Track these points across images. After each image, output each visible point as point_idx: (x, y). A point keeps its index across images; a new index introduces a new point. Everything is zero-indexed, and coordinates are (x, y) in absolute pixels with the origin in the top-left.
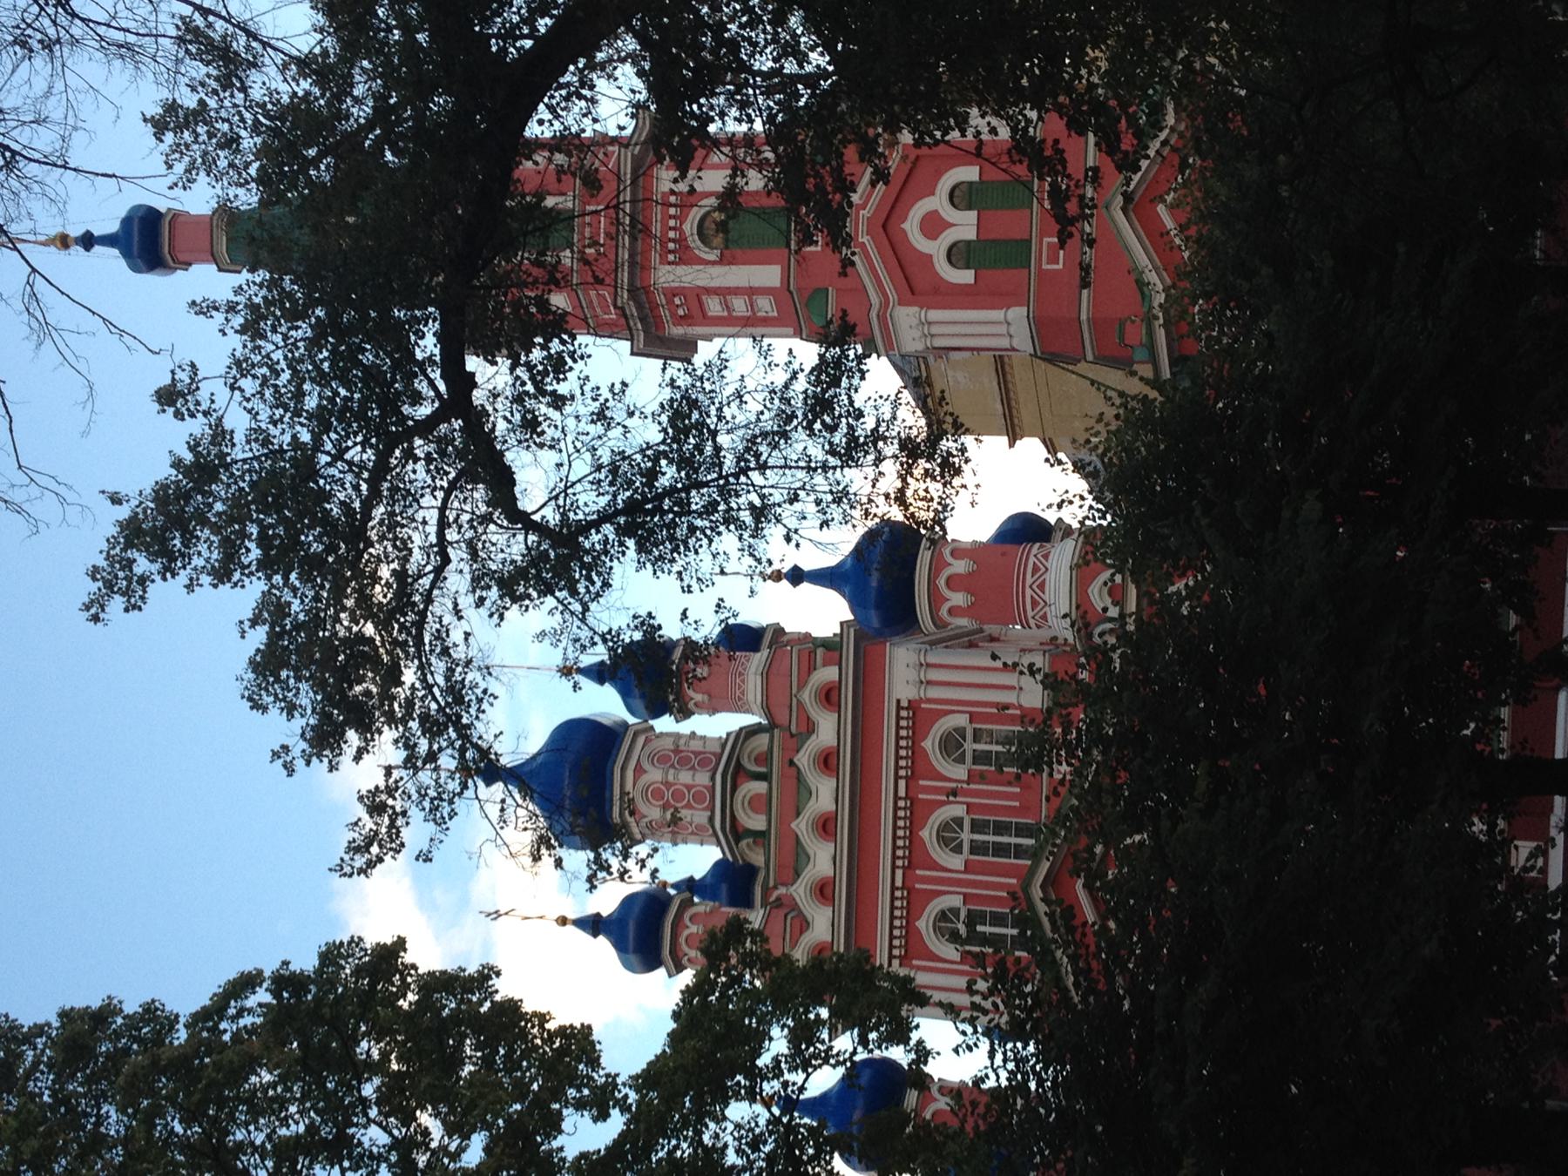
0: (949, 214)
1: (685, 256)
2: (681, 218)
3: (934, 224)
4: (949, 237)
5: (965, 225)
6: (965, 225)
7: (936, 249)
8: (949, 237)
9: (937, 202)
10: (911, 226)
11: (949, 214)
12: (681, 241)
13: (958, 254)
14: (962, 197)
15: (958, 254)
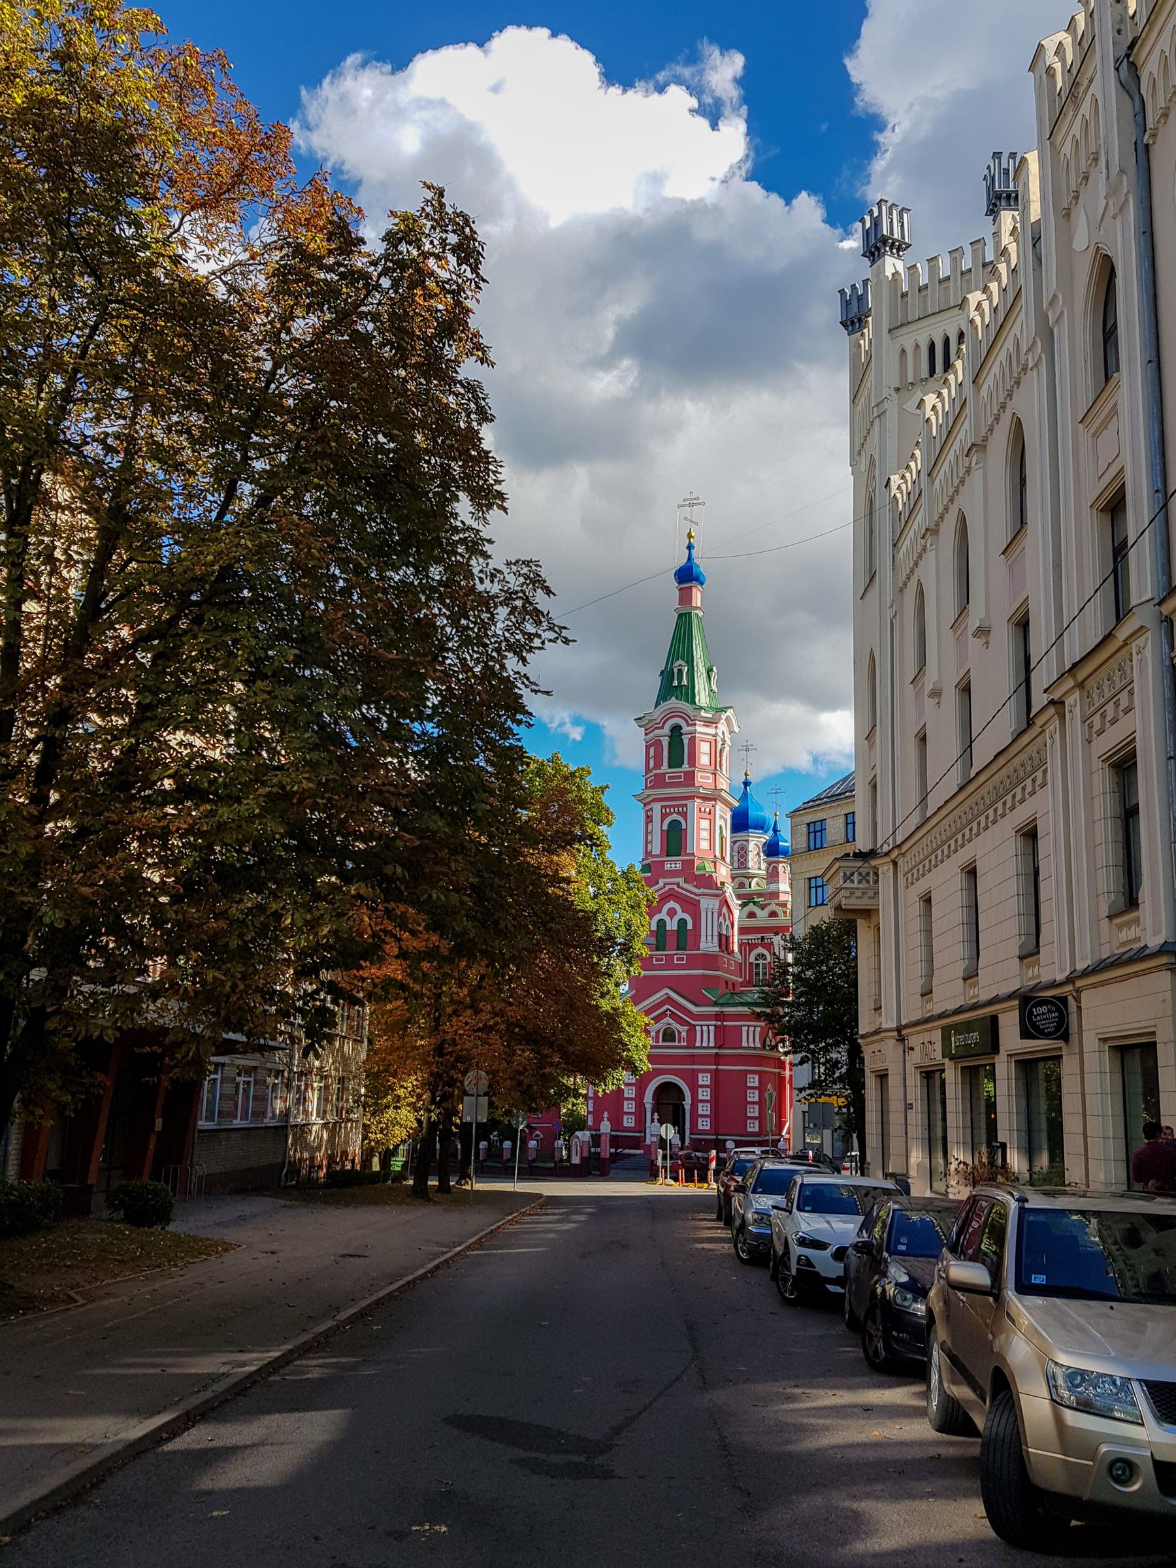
0: (676, 918)
1: (664, 816)
2: (678, 813)
3: (672, 913)
4: (667, 919)
5: (672, 925)
6: (672, 925)
7: (663, 915)
8: (667, 919)
9: (680, 914)
10: (672, 904)
11: (676, 918)
12: (671, 814)
13: (661, 923)
14: (682, 922)
15: (661, 923)
